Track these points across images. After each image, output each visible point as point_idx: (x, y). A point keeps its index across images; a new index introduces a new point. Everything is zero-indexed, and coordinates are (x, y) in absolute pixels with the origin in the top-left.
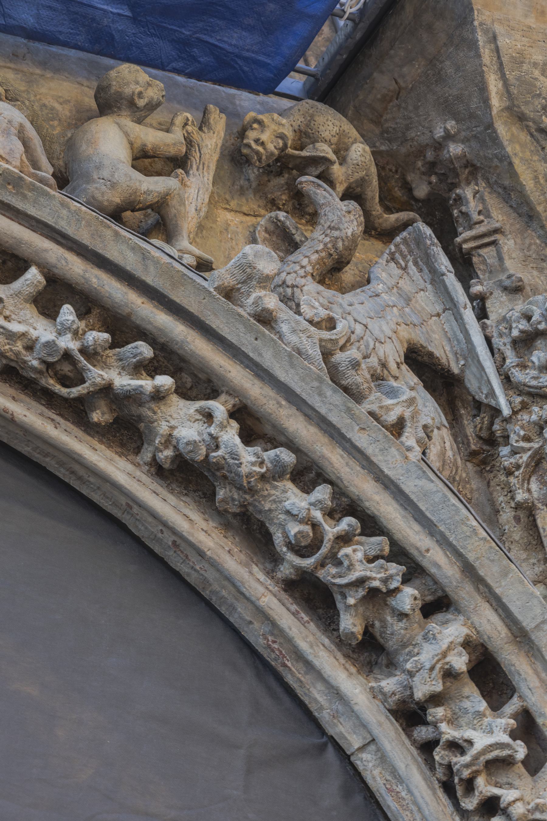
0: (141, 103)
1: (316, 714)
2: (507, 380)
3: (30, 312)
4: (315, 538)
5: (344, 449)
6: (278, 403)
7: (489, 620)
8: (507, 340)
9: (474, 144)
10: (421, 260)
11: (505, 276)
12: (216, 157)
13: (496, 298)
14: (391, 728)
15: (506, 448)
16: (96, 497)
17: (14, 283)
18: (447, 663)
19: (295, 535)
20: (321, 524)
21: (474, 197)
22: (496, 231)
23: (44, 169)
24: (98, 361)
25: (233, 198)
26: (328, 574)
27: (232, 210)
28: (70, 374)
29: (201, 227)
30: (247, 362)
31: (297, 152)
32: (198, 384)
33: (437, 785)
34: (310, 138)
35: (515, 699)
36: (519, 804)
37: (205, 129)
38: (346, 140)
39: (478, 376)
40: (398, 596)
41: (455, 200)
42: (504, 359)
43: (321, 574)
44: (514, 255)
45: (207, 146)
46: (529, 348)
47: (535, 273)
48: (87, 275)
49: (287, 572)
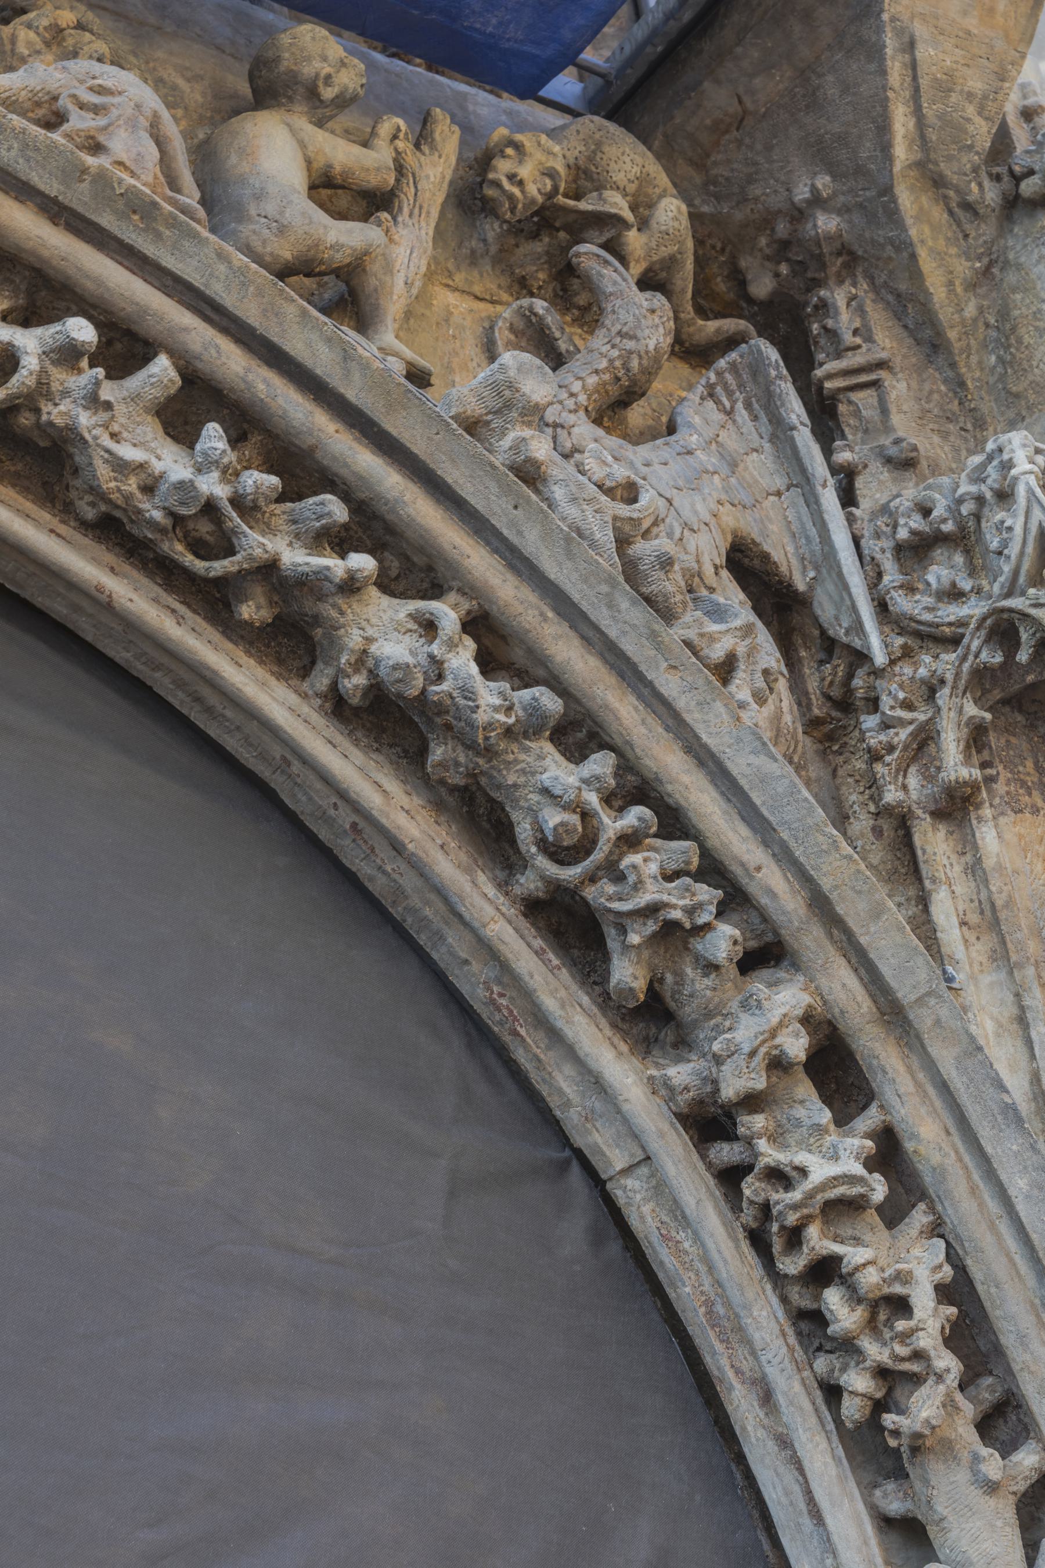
0: (328, 93)
1: (558, 1113)
2: (882, 607)
3: (151, 429)
4: (584, 836)
5: (640, 697)
6: (542, 614)
7: (844, 985)
8: (888, 544)
9: (857, 218)
10: (758, 401)
11: (890, 440)
12: (440, 198)
13: (872, 475)
14: (678, 1142)
15: (872, 717)
16: (231, 743)
17: (128, 379)
18: (776, 1047)
19: (555, 828)
20: (597, 813)
21: (848, 305)
22: (881, 365)
23: (186, 191)
24: (257, 521)
25: (458, 268)
26: (602, 895)
27: (456, 289)
28: (208, 537)
29: (408, 314)
30: (496, 543)
31: (571, 203)
32: (415, 573)
33: (741, 1235)
34: (592, 180)
35: (873, 1110)
36: (871, 1269)
37: (425, 148)
38: (650, 191)
39: (837, 598)
40: (708, 936)
41: (816, 307)
42: (880, 575)
43: (590, 893)
44: (905, 408)
45: (428, 177)
46: (920, 561)
47: (936, 439)
48: (250, 377)
49: (532, 886)
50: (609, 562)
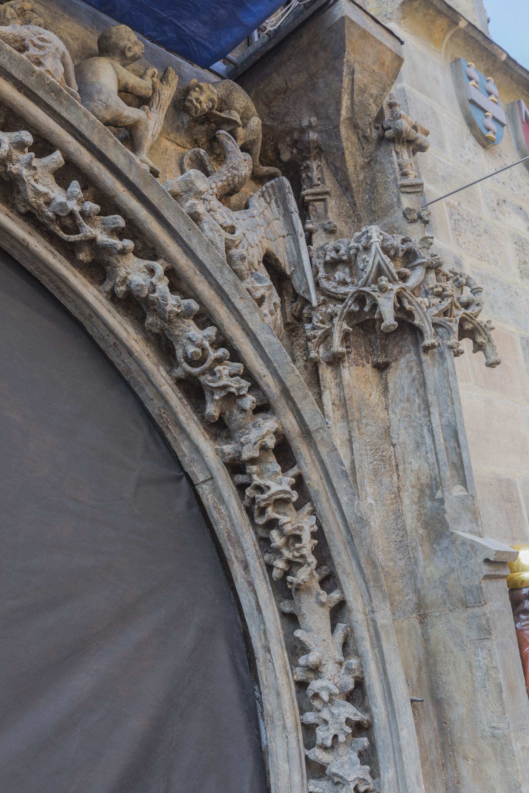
0: (129, 54)
1: (180, 459)
2: (317, 284)
3: (50, 180)
4: (202, 357)
5: (228, 308)
6: (195, 272)
7: (290, 422)
8: (322, 261)
9: (324, 135)
10: (280, 200)
11: (327, 222)
12: (168, 103)
13: (319, 234)
14: (224, 473)
15: (309, 325)
16: (70, 307)
17: (43, 158)
18: (264, 442)
19: (192, 353)
20: (208, 349)
21: (317, 168)
22: (327, 193)
23: (73, 86)
24: (89, 222)
25: (172, 132)
26: (206, 380)
27: (170, 140)
28: (69, 225)
29: (152, 147)
30: (180, 242)
31: (219, 113)
32: (148, 250)
33: (243, 509)
34: (227, 105)
35: (296, 468)
36: (289, 525)
37: (164, 83)
38: (248, 113)
39: (301, 279)
40: (244, 399)
41: (305, 167)
42: (318, 272)
43: (202, 379)
44: (334, 211)
45: (164, 94)
46: (333, 269)
47: (343, 224)
48: (92, 165)
49: (180, 374)
50: (222, 256)
